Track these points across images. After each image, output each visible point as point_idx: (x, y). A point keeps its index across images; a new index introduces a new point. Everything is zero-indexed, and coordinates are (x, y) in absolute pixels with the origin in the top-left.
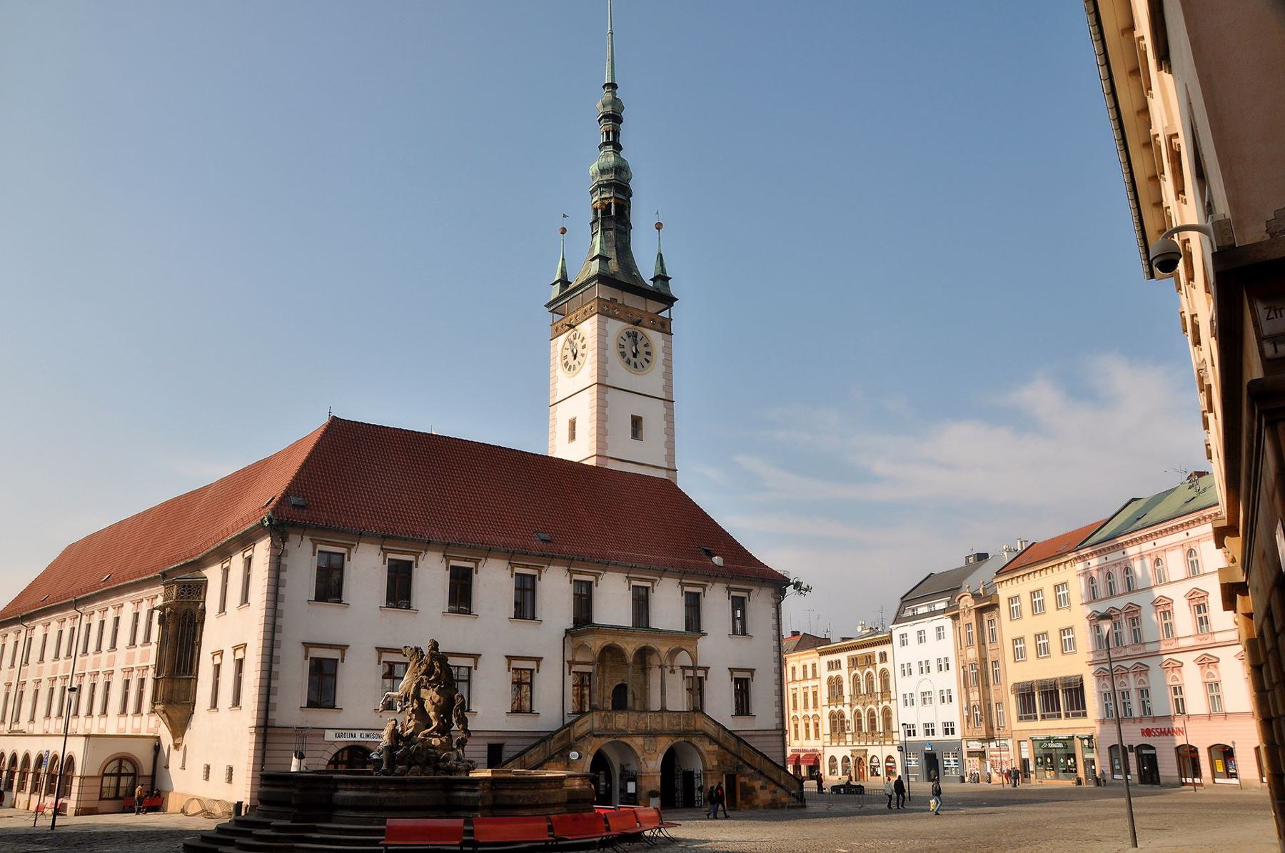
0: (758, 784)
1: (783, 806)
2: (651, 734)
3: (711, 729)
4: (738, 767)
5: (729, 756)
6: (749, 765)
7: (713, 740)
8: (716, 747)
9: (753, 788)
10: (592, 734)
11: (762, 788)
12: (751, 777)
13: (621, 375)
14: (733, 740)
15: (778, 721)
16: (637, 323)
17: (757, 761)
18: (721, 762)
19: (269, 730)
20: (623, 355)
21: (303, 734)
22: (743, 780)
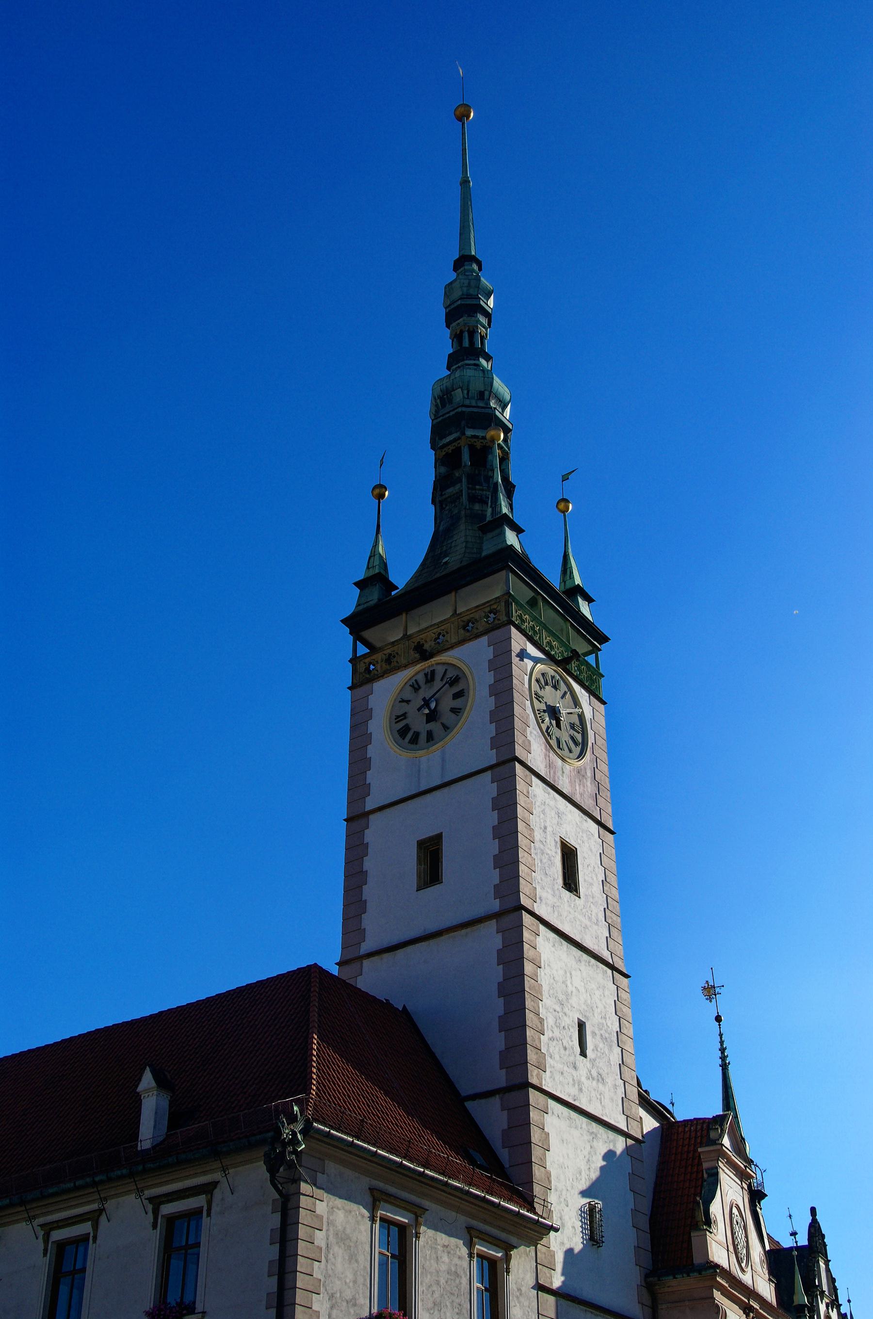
16: (425, 655)
20: (403, 732)
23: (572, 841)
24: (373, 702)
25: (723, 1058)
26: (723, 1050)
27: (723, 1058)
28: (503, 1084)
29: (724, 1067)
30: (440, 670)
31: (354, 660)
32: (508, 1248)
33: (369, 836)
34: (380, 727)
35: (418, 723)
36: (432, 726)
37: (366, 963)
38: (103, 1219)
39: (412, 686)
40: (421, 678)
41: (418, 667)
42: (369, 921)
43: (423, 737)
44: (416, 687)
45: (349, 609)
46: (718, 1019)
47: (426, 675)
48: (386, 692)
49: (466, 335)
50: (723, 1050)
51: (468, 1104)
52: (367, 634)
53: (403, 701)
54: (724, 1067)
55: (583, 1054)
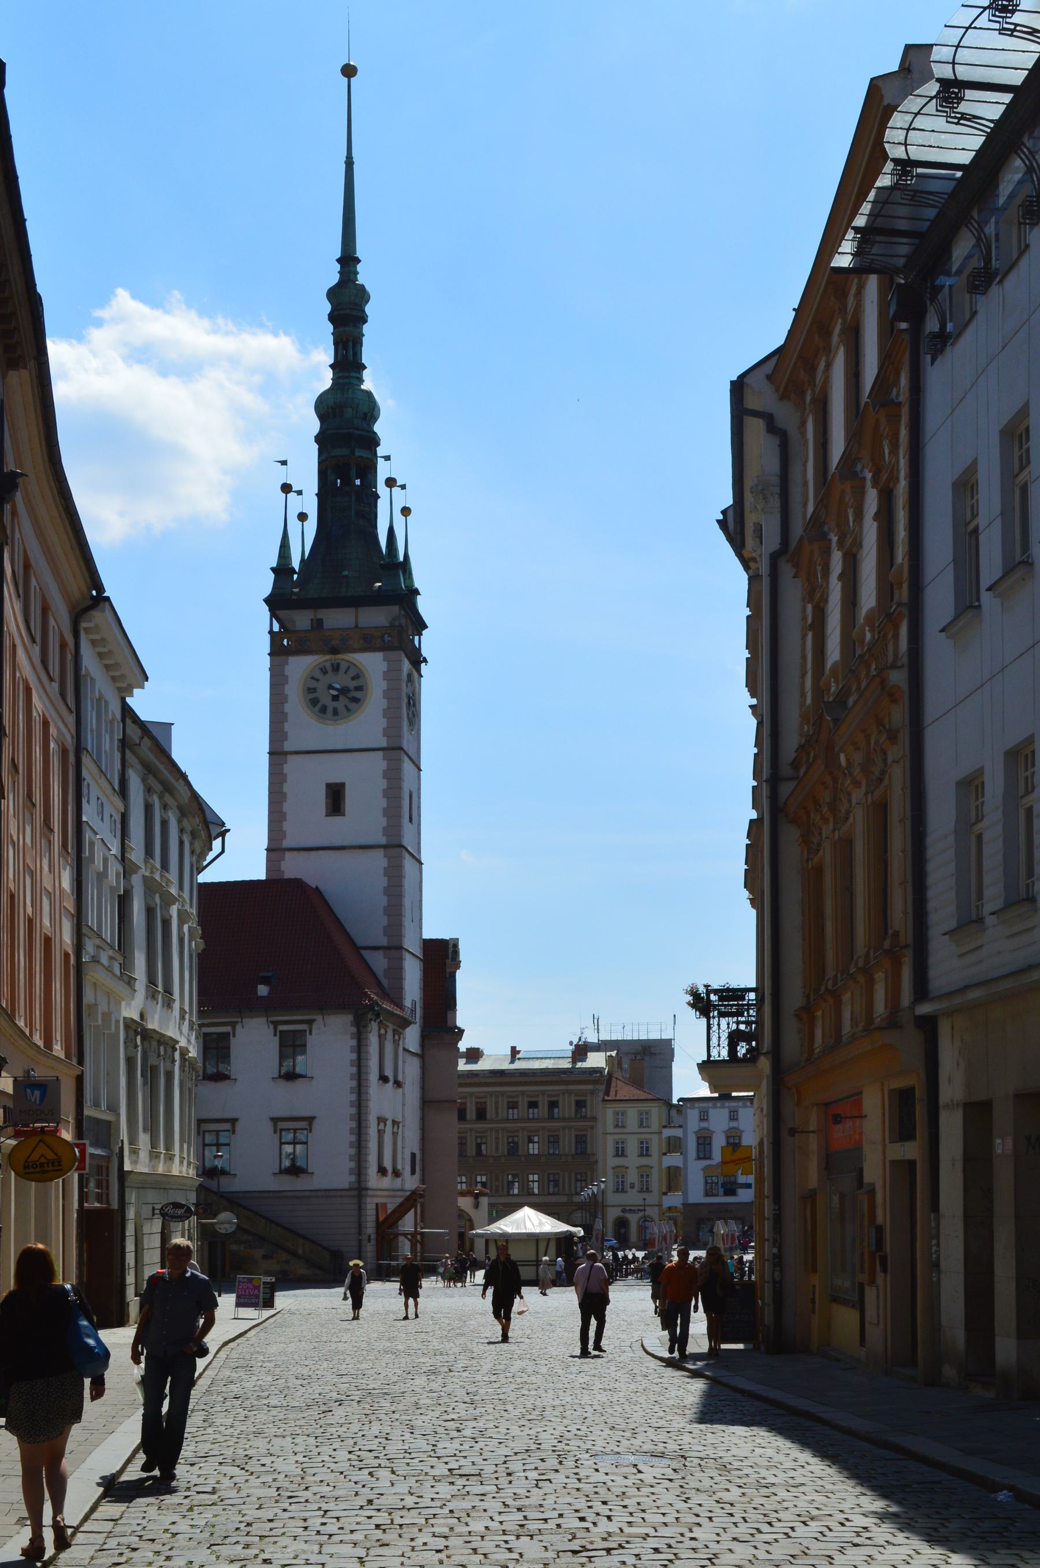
0: (258, 1253)
11: (265, 1257)
13: (307, 729)
15: (353, 1178)
16: (334, 651)
20: (314, 702)
22: (234, 1247)
24: (288, 670)
30: (343, 666)
31: (271, 632)
33: (287, 768)
34: (294, 690)
35: (326, 699)
36: (335, 704)
39: (321, 669)
40: (328, 666)
41: (328, 657)
43: (330, 711)
44: (324, 671)
45: (267, 588)
47: (333, 665)
48: (300, 666)
49: (351, 344)
52: (278, 612)
53: (313, 678)
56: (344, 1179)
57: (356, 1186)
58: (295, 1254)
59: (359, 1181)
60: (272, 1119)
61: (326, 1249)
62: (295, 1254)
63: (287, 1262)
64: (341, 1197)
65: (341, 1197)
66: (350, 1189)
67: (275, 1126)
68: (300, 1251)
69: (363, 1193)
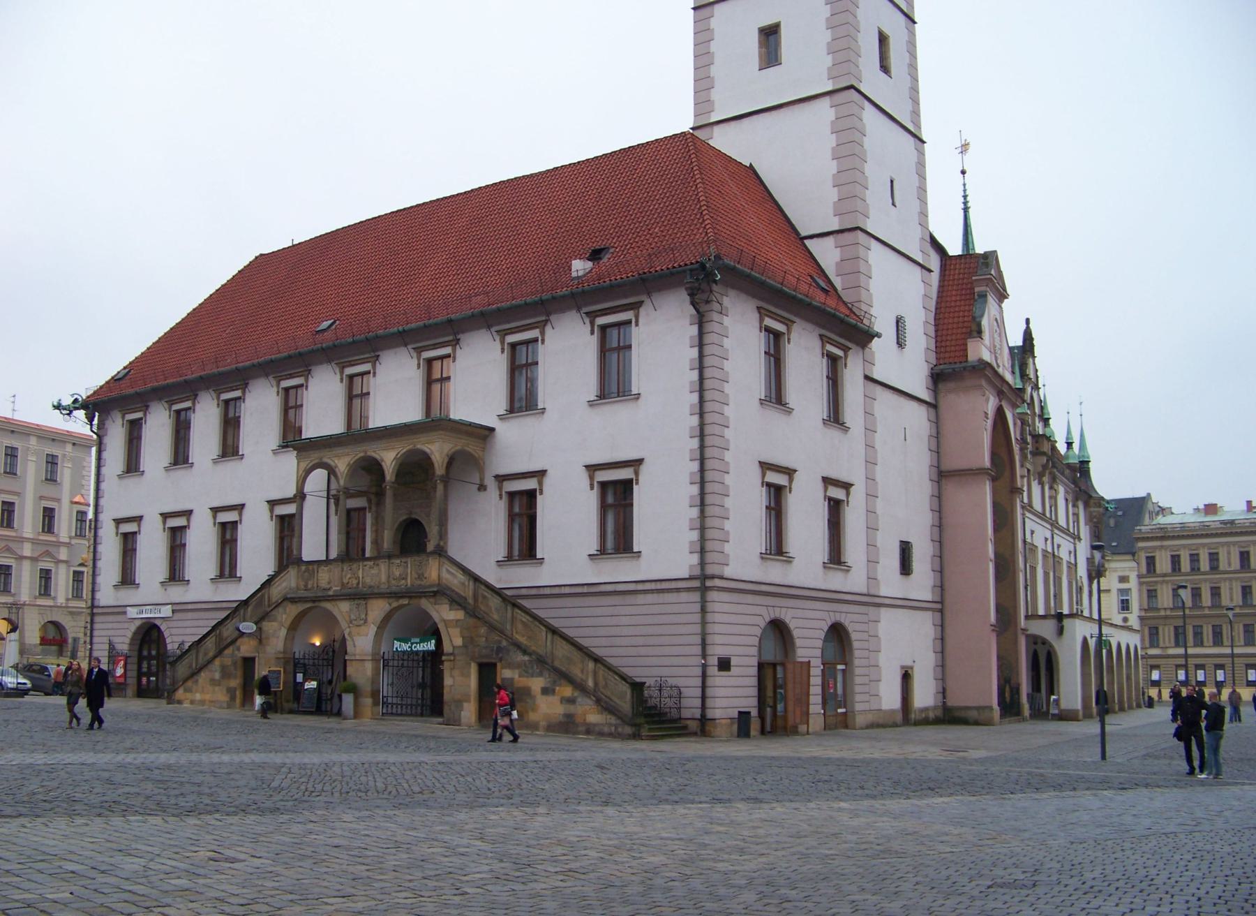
1: (589, 730)
2: (360, 596)
3: (455, 580)
4: (499, 649)
5: (483, 630)
6: (518, 646)
7: (456, 601)
8: (459, 615)
9: (527, 692)
10: (288, 599)
11: (545, 691)
12: (526, 671)
14: (495, 602)
15: (695, 559)
17: (542, 643)
18: (469, 641)
19: (95, 611)
21: (120, 610)
23: (886, 30)
25: (965, 203)
26: (965, 197)
27: (965, 203)
28: (837, 228)
29: (966, 210)
32: (846, 350)
33: (714, 23)
37: (716, 129)
38: (548, 329)
42: (715, 95)
46: (963, 172)
50: (965, 197)
51: (807, 242)
54: (966, 210)
55: (894, 204)
56: (681, 563)
57: (697, 572)
58: (580, 687)
59: (703, 563)
60: (586, 466)
61: (623, 678)
62: (580, 687)
63: (571, 701)
64: (678, 590)
65: (678, 590)
66: (691, 578)
67: (591, 478)
68: (590, 683)
69: (709, 583)
